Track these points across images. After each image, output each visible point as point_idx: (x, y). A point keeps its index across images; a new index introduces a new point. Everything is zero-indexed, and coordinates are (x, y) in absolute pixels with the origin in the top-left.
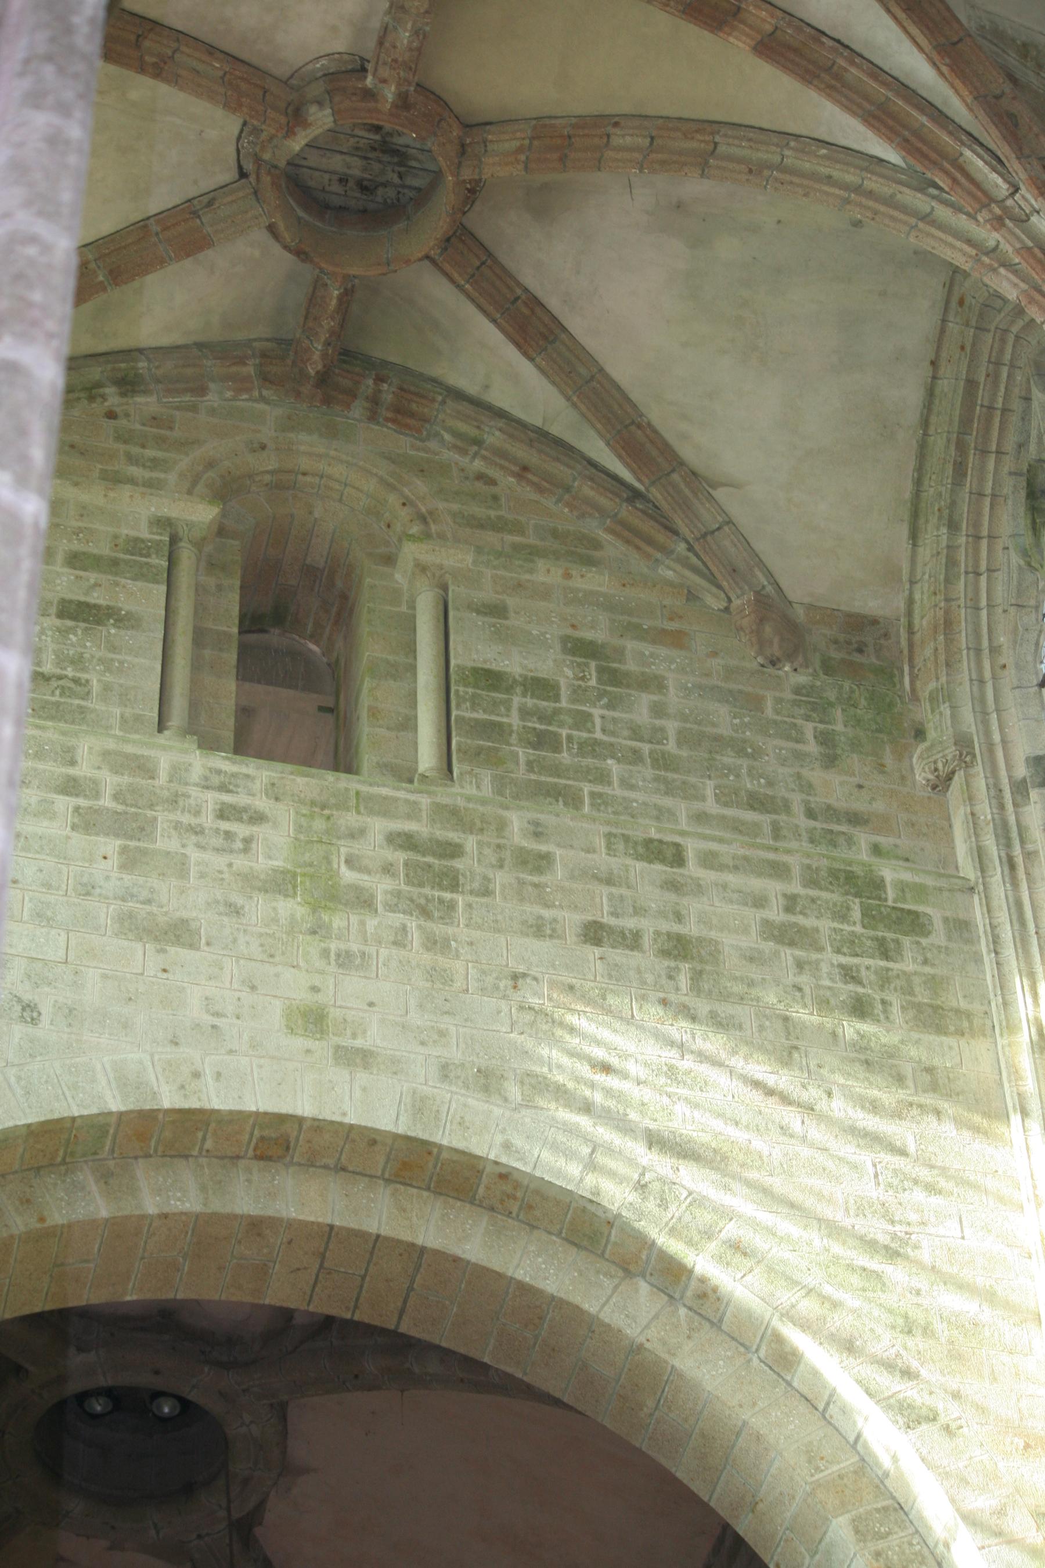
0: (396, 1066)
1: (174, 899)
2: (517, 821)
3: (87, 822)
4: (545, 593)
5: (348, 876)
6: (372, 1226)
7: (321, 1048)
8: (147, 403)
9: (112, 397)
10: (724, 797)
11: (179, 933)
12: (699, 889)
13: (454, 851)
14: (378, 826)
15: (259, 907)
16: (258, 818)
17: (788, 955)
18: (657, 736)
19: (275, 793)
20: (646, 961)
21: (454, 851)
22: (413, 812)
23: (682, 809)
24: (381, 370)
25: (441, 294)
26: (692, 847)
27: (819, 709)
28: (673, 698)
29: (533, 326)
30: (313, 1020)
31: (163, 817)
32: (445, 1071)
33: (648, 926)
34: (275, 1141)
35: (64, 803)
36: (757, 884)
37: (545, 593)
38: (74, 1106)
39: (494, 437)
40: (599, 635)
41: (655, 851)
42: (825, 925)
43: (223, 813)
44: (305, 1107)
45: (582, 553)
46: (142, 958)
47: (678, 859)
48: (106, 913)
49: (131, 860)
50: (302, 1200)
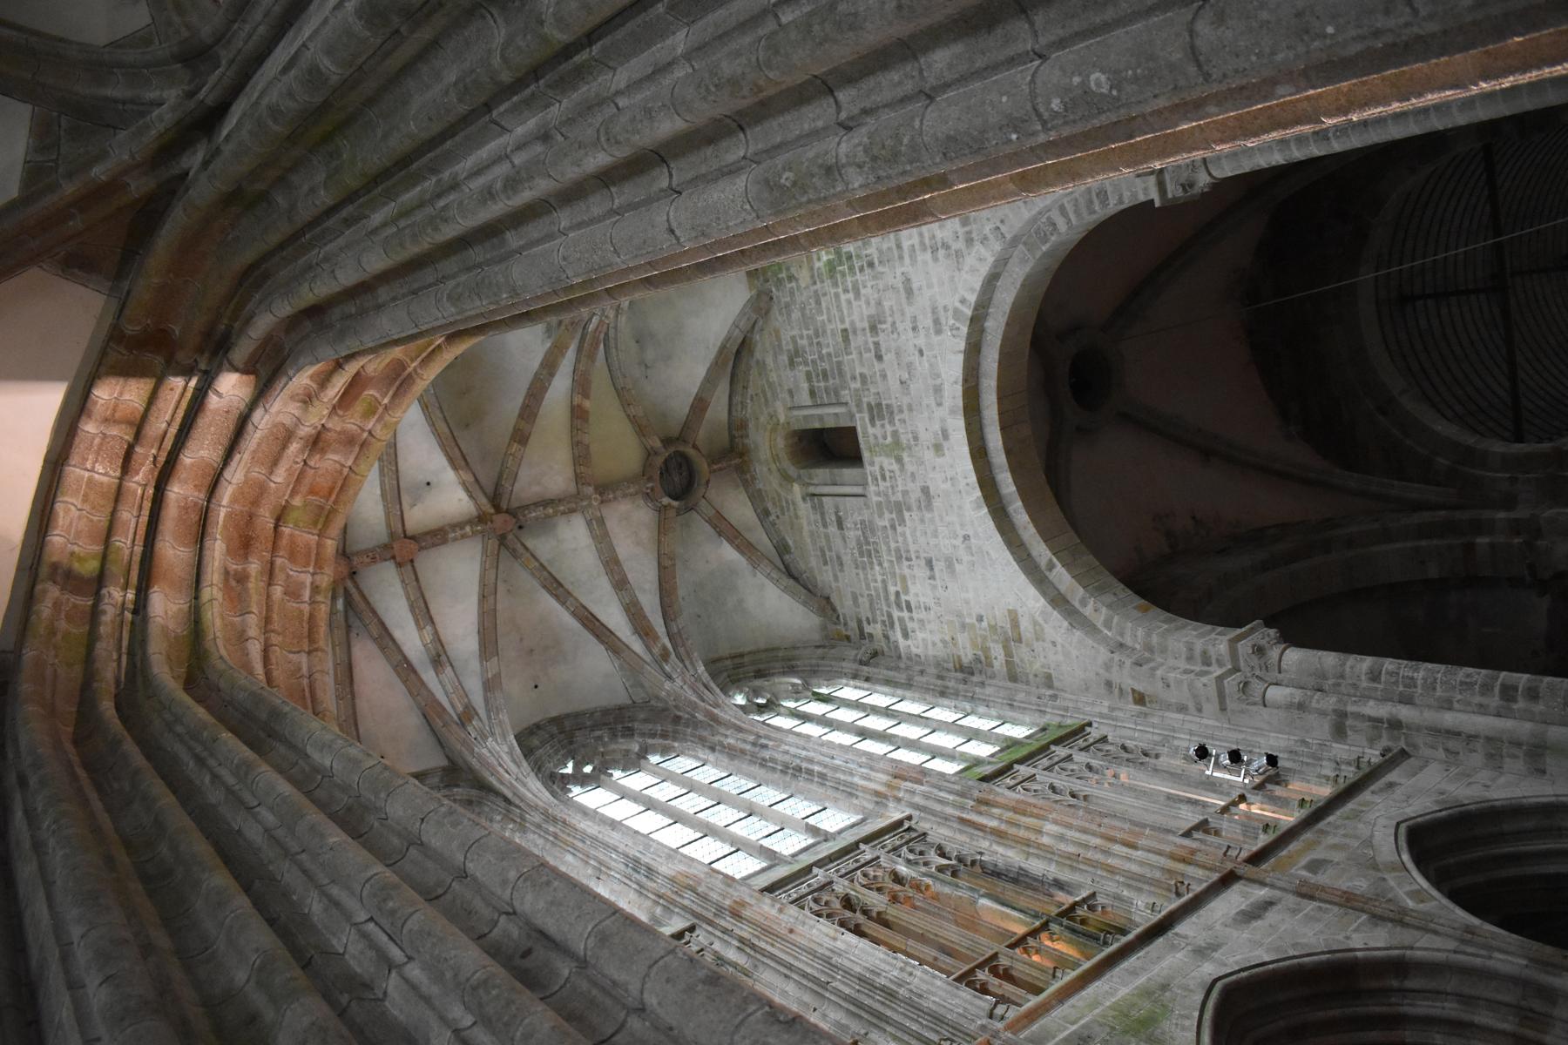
0: (943, 420)
1: (916, 494)
2: (853, 385)
3: (902, 522)
4: (779, 376)
5: (889, 439)
6: (996, 417)
7: (946, 445)
8: (770, 506)
9: (772, 517)
10: (820, 312)
11: (925, 490)
12: (852, 323)
13: (869, 405)
14: (871, 430)
15: (910, 468)
16: (882, 468)
17: (863, 291)
18: (809, 337)
19: (872, 464)
20: (881, 338)
21: (869, 405)
22: (862, 419)
23: (829, 327)
24: (732, 438)
25: (702, 435)
26: (841, 327)
27: (780, 281)
28: (795, 332)
29: (700, 405)
30: (938, 448)
31: (893, 499)
32: (939, 404)
33: (871, 340)
34: (979, 453)
35: (899, 529)
36: (844, 304)
37: (779, 376)
38: (991, 524)
39: (737, 399)
40: (785, 358)
41: (846, 339)
42: (849, 279)
43: (884, 478)
44: (966, 449)
45: (762, 365)
46: (937, 503)
47: (845, 330)
48: (928, 516)
49: (909, 509)
50: (994, 439)
